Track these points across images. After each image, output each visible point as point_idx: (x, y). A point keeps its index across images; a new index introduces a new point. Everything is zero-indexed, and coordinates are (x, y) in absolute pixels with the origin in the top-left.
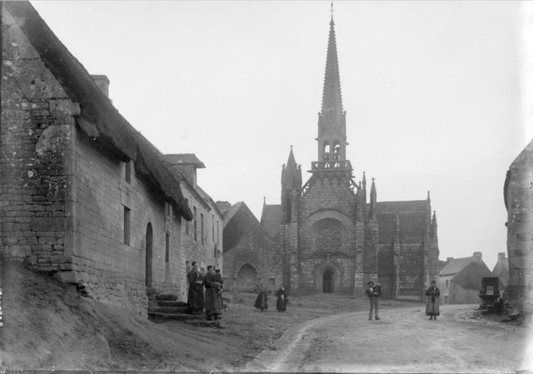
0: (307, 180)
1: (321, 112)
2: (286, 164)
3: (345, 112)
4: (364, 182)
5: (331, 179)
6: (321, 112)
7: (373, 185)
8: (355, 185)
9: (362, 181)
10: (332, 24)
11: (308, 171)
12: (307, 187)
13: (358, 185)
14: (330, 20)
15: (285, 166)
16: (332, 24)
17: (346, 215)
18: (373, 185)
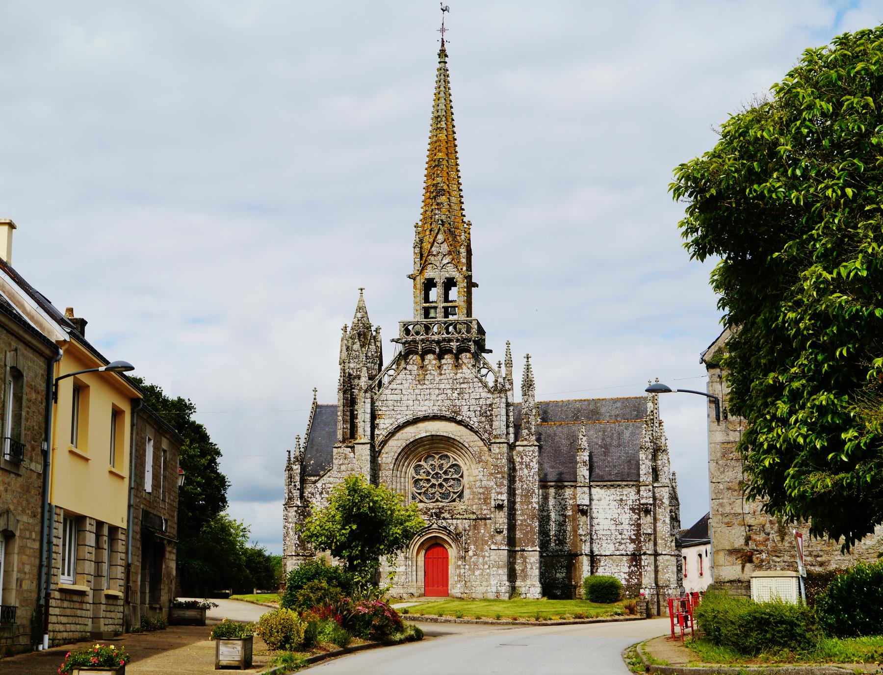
0: (392, 358)
1: (420, 224)
2: (350, 325)
3: (469, 224)
4: (509, 364)
5: (440, 357)
6: (420, 224)
7: (528, 368)
8: (490, 370)
9: (503, 362)
10: (443, 54)
11: (393, 340)
12: (391, 372)
13: (495, 367)
14: (439, 47)
15: (349, 329)
16: (443, 54)
17: (471, 429)
18: (528, 368)
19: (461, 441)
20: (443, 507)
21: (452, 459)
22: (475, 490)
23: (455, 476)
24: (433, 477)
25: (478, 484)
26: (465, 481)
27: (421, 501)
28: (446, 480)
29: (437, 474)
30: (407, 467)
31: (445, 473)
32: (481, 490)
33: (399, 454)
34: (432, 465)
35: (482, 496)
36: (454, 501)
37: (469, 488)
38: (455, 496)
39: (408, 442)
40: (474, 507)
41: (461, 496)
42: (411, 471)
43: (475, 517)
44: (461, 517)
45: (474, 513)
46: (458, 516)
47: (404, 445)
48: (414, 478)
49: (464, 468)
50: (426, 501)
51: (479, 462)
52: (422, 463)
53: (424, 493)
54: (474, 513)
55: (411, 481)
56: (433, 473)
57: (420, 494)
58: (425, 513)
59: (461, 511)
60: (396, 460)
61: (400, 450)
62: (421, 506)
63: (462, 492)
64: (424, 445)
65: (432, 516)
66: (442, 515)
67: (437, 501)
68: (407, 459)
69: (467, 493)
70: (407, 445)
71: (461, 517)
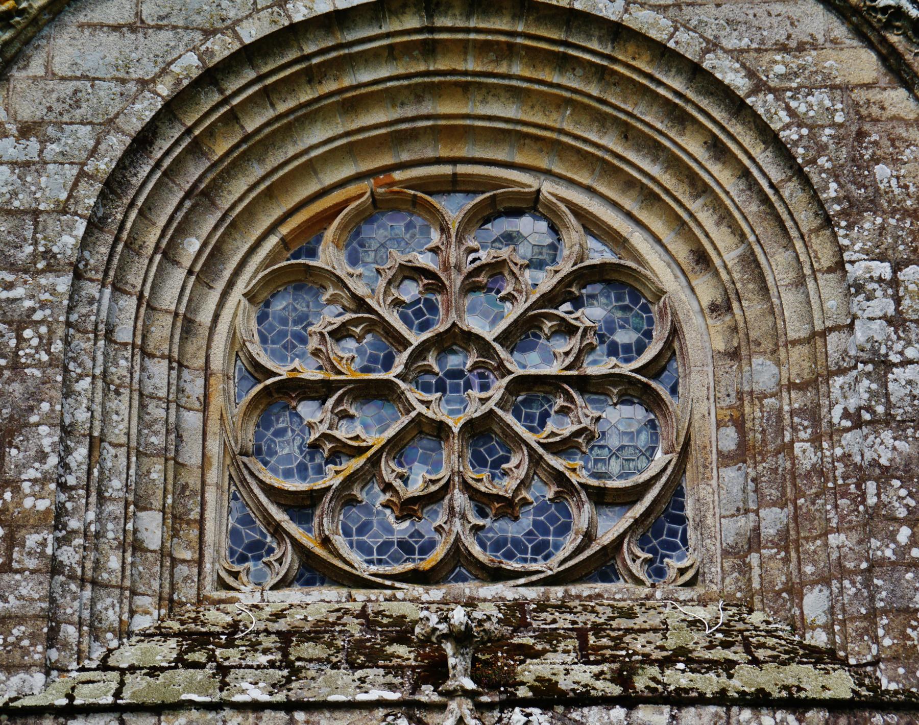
19: (687, 44)
20: (516, 615)
21: (573, 235)
22: (806, 455)
23: (600, 365)
24: (415, 371)
25: (847, 395)
26: (699, 393)
27: (314, 570)
28: (531, 391)
29: (457, 339)
30: (204, 273)
31: (521, 334)
32: (886, 448)
33: (143, 141)
34: (411, 272)
35: (899, 498)
36: (603, 565)
37: (743, 453)
38: (611, 527)
39: (221, 48)
40: (815, 603)
41: (664, 523)
42: (230, 316)
43: (841, 685)
44: (709, 683)
45: (816, 656)
46: (678, 678)
47: (189, 64)
48: (259, 371)
49: (687, 297)
50: (364, 570)
51: (854, 210)
52: (329, 256)
53: (345, 498)
54: (818, 657)
55: (232, 400)
56: (416, 339)
57: (302, 506)
58: (364, 655)
59: (696, 641)
60: (113, 186)
61: (145, 109)
62: (319, 601)
63: (674, 494)
64: (352, 103)
65: (434, 671)
66: (531, 671)
67: (458, 563)
68: (203, 196)
69: (717, 501)
70: (211, 77)
71: (709, 683)
